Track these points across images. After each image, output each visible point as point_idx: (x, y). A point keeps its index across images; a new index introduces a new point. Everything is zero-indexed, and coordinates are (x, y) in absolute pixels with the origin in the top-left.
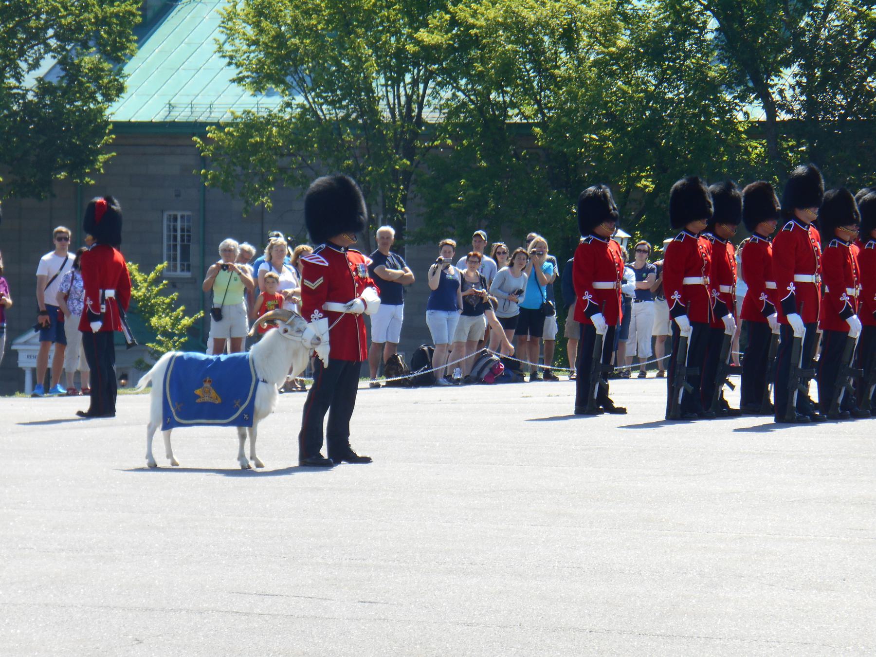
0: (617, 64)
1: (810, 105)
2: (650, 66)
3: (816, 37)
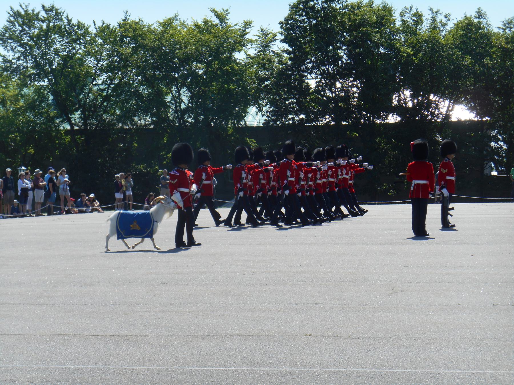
0: (20, 111)
1: (85, 124)
2: (31, 112)
3: (85, 102)
